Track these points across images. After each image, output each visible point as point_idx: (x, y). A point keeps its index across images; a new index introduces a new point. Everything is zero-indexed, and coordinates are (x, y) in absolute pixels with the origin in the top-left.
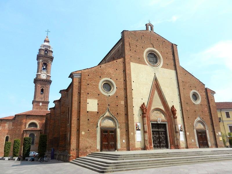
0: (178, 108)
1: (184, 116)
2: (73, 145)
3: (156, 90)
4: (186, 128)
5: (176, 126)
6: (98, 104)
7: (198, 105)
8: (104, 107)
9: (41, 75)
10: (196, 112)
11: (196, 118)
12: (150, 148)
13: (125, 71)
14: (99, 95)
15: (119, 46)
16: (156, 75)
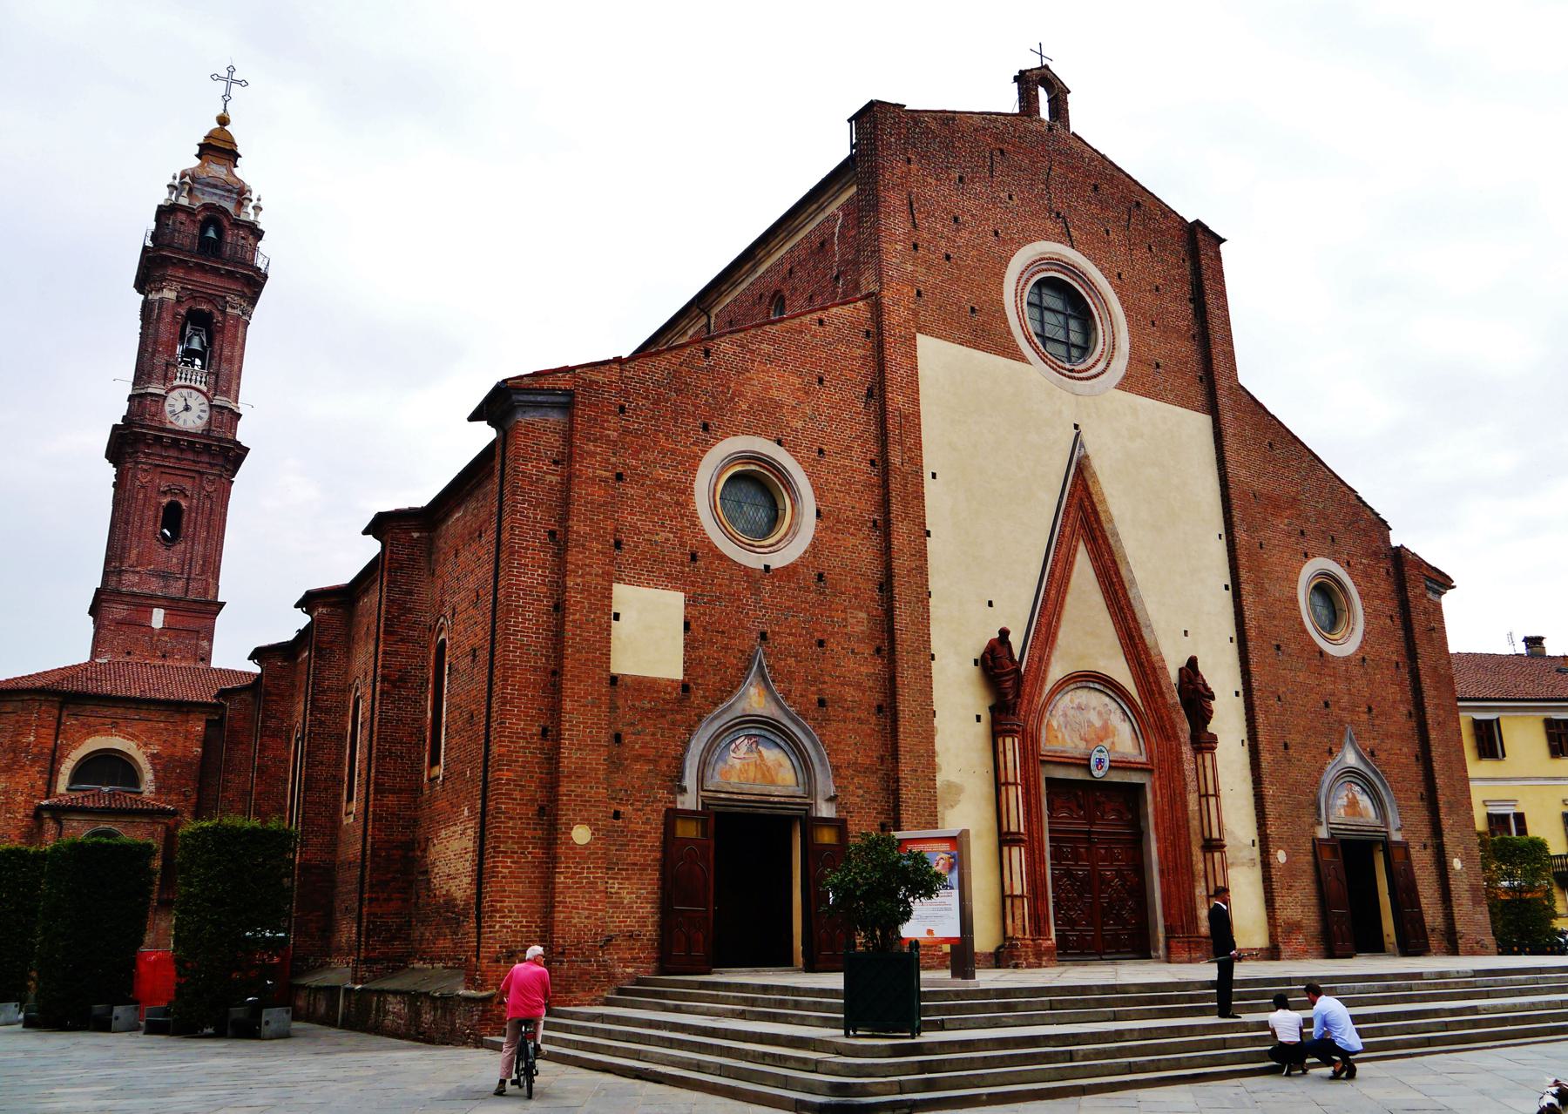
0: (1222, 677)
1: (1262, 737)
2: (508, 922)
3: (1082, 548)
4: (1270, 820)
5: (1212, 801)
6: (687, 626)
7: (1347, 660)
8: (726, 648)
9: (169, 401)
10: (1334, 709)
11: (1330, 752)
12: (1039, 954)
13: (876, 393)
14: (694, 557)
15: (833, 208)
16: (1086, 437)
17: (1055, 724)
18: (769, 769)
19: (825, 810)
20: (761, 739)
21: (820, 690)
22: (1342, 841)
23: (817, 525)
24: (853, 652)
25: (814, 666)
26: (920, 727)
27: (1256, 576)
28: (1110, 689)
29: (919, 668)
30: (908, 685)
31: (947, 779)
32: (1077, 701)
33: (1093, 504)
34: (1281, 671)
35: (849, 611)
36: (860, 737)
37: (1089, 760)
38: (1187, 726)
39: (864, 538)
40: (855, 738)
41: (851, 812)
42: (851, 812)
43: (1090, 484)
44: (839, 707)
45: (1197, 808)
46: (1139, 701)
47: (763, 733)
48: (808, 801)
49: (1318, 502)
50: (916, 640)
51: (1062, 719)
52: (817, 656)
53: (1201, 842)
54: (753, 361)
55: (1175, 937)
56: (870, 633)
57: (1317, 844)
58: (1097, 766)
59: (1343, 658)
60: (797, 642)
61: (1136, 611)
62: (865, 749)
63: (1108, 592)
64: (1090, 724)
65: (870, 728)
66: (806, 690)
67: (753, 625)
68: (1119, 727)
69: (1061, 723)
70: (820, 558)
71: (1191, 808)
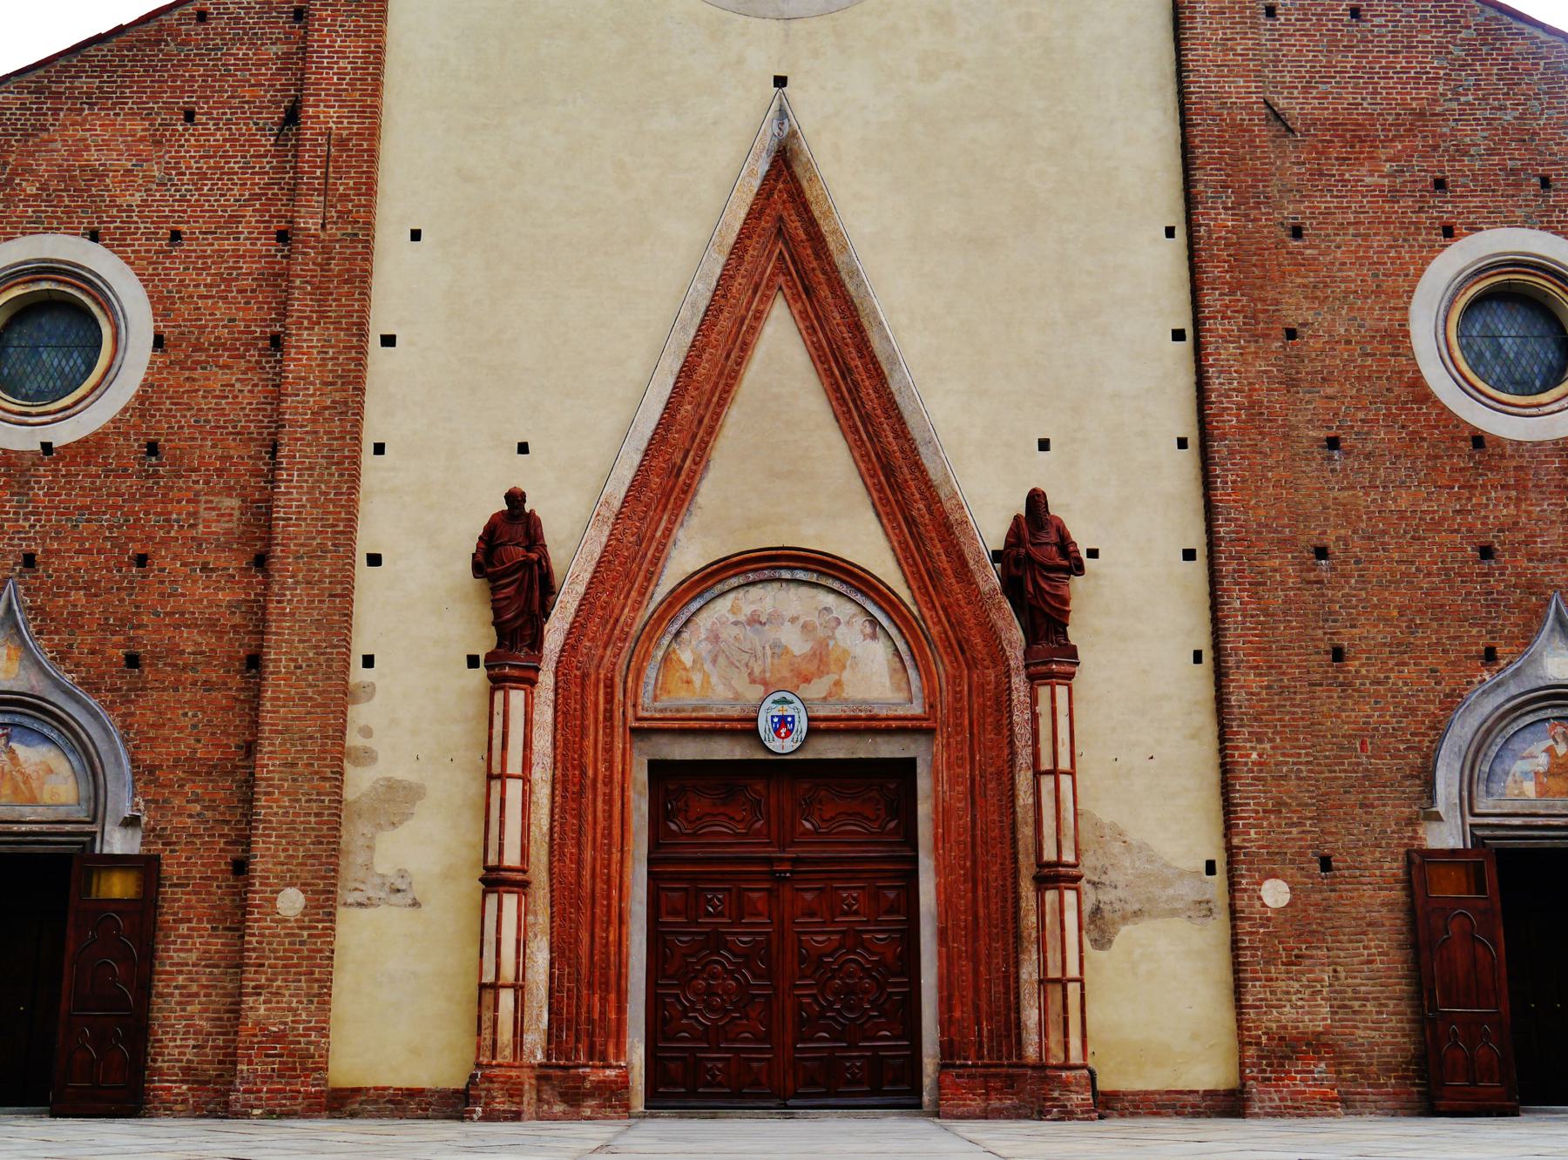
11: (1490, 656)
17: (686, 657)
18: (27, 779)
19: (119, 842)
20: (18, 729)
21: (131, 639)
22: (1501, 853)
23: (152, 362)
24: (205, 568)
25: (122, 600)
28: (835, 578)
32: (747, 610)
33: (811, 224)
34: (1336, 493)
35: (203, 498)
36: (204, 712)
37: (756, 720)
38: (1017, 635)
39: (248, 369)
40: (195, 716)
41: (175, 843)
42: (175, 843)
43: (805, 184)
44: (165, 664)
45: (1030, 801)
46: (905, 594)
47: (17, 719)
48: (87, 828)
49: (1502, 108)
51: (705, 647)
52: (130, 582)
53: (1034, 870)
54: (56, 111)
55: (954, 1066)
56: (244, 532)
57: (1421, 863)
58: (777, 732)
59: (1556, 442)
60: (93, 563)
62: (213, 734)
63: (839, 387)
64: (779, 650)
65: (226, 697)
66: (102, 642)
67: (9, 545)
68: (858, 651)
69: (704, 654)
70: (154, 416)
71: (1020, 802)
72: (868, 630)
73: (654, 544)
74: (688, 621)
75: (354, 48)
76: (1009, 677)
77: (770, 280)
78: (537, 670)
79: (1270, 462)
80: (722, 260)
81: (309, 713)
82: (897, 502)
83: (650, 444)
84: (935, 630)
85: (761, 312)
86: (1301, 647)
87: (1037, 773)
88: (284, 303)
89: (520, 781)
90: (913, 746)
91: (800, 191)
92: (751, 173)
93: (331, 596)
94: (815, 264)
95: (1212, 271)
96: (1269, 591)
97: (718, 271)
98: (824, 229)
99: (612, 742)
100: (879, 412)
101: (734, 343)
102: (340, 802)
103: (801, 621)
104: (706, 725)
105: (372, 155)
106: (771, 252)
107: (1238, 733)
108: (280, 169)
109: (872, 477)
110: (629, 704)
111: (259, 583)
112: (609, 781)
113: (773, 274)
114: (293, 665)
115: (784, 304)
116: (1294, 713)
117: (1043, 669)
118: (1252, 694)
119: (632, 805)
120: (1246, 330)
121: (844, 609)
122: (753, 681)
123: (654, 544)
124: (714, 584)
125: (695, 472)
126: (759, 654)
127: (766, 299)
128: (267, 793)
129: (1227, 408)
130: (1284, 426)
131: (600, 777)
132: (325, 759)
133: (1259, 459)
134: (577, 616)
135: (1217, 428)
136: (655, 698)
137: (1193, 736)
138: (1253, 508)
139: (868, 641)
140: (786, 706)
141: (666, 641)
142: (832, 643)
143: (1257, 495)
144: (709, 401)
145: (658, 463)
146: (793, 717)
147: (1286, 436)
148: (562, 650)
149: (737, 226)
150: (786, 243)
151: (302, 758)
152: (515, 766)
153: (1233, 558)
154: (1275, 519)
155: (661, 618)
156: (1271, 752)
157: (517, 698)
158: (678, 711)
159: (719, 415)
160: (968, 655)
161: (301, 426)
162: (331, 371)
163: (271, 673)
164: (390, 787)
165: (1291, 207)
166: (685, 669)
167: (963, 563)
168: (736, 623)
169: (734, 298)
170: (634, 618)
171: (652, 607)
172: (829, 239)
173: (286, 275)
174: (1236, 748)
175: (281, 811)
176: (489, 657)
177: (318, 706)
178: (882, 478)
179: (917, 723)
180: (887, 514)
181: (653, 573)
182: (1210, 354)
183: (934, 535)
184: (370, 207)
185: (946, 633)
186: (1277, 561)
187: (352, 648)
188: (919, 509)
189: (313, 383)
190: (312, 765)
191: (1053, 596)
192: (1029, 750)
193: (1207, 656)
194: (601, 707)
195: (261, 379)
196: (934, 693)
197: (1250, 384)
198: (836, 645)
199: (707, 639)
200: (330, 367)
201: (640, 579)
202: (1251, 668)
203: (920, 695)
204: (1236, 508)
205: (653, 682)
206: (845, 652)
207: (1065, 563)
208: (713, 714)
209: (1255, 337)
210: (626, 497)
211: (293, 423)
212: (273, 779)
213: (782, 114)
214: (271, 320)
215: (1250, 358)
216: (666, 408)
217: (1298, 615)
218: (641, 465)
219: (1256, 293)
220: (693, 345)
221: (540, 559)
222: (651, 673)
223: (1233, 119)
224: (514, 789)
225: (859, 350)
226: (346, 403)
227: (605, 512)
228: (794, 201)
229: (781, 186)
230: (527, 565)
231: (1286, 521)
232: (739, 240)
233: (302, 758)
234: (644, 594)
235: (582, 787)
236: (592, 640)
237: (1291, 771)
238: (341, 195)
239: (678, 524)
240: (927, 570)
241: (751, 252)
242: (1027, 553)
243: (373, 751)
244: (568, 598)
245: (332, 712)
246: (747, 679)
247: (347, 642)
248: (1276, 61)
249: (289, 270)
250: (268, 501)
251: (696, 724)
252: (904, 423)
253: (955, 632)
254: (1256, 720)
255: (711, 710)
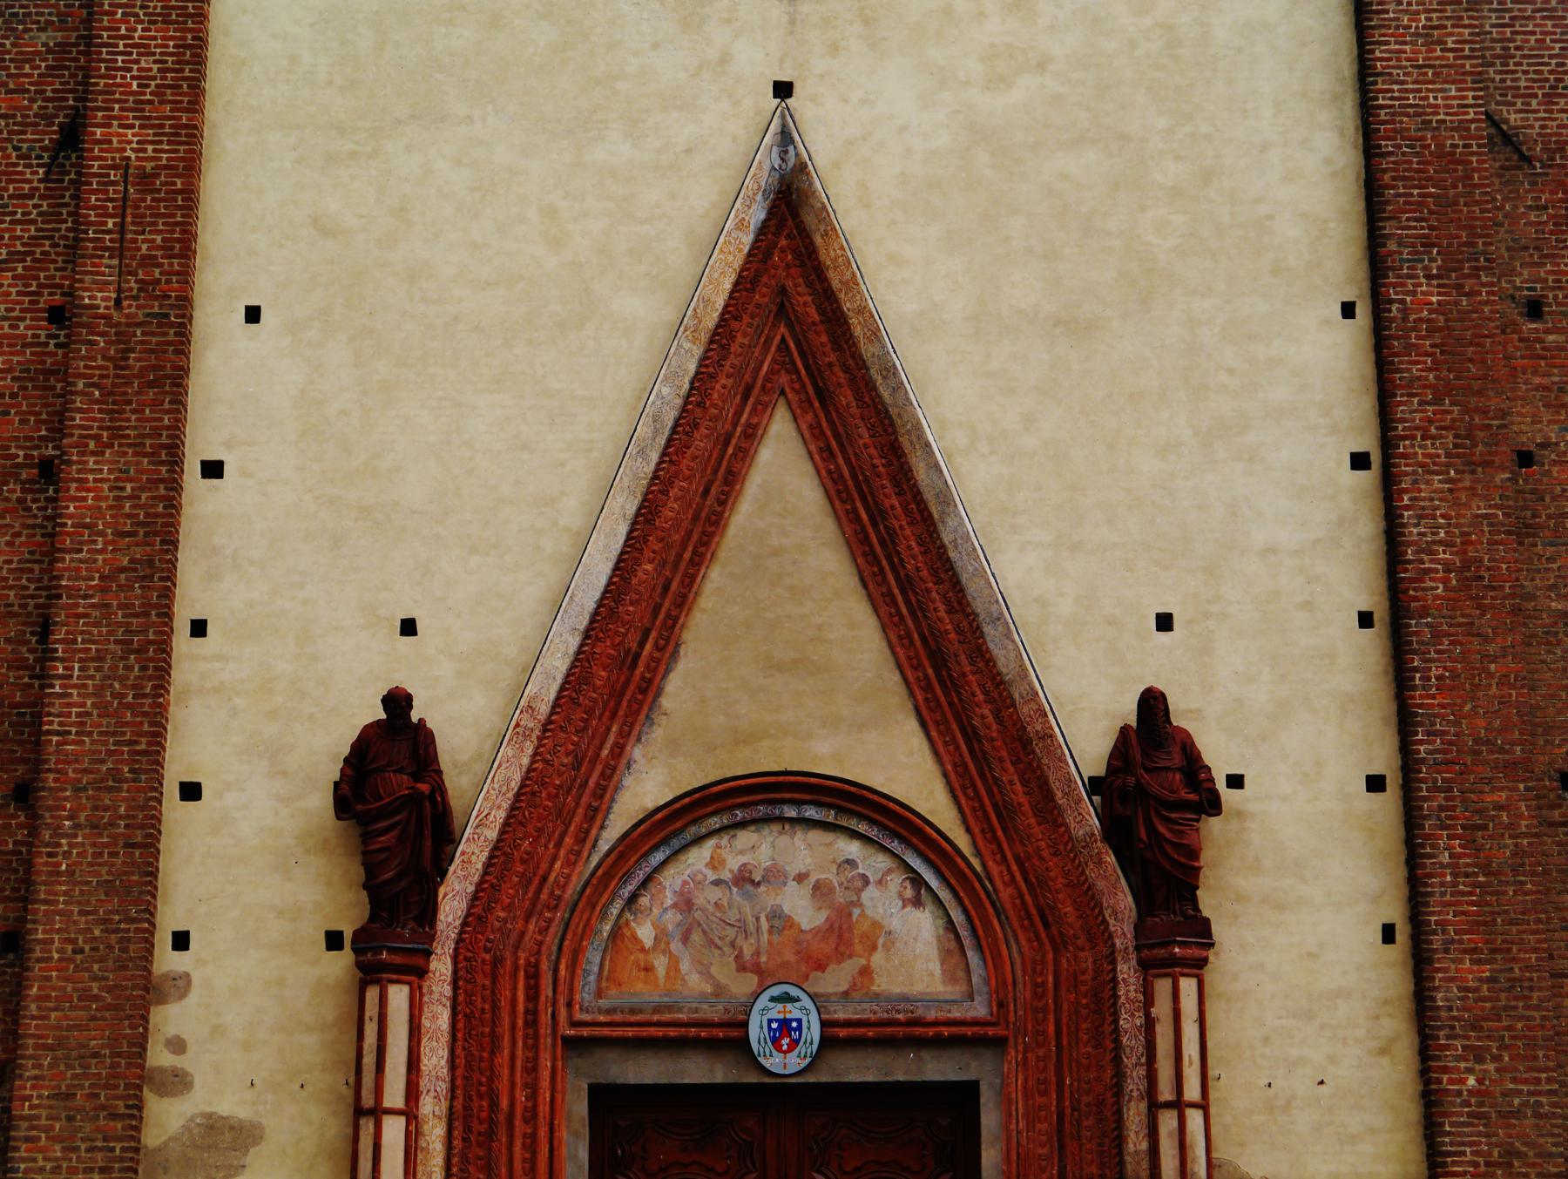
17: (645, 932)
26: (95, 978)
27: (1466, 410)
28: (861, 817)
29: (112, 825)
30: (70, 873)
31: (209, 1109)
32: (734, 863)
37: (744, 1025)
38: (1125, 901)
43: (818, 240)
45: (1144, 1146)
46: (962, 841)
50: (110, 753)
51: (671, 919)
58: (776, 1043)
61: (964, 578)
63: (866, 540)
64: (780, 921)
68: (895, 924)
71: (1131, 1148)
72: (909, 893)
73: (599, 768)
74: (648, 879)
75: (164, 41)
76: (1114, 962)
77: (767, 379)
78: (428, 954)
79: (1492, 649)
80: (698, 351)
81: (93, 1018)
82: (951, 704)
83: (592, 621)
84: (1006, 894)
85: (755, 427)
86: (1539, 921)
87: (1154, 1107)
88: (61, 413)
89: (402, 1121)
90: (974, 1064)
91: (812, 250)
92: (741, 225)
93: (128, 845)
94: (832, 358)
95: (1412, 368)
96: (1491, 837)
97: (692, 367)
98: (847, 306)
99: (536, 1059)
100: (925, 574)
101: (715, 472)
102: (137, 1150)
103: (812, 879)
104: (673, 1032)
105: (188, 200)
106: (769, 340)
107: (1447, 1047)
108: (53, 216)
109: (915, 668)
110: (562, 1001)
111: (20, 826)
112: (531, 1116)
113: (771, 371)
114: (70, 947)
115: (788, 415)
116: (1528, 1018)
117: (1161, 952)
118: (1467, 989)
119: (565, 1151)
120: (1458, 456)
121: (874, 863)
122: (742, 968)
123: (599, 768)
124: (686, 826)
125: (658, 661)
126: (751, 928)
127: (763, 409)
128: (28, 1139)
129: (1430, 570)
130: (1512, 596)
131: (518, 1116)
132: (116, 1087)
133: (1476, 644)
134: (486, 873)
135: (1416, 599)
136: (599, 993)
137: (1383, 1052)
138: (1468, 716)
139: (909, 909)
140: (789, 1006)
141: (615, 910)
142: (856, 912)
143: (1473, 698)
144: (679, 556)
145: (605, 648)
146: (799, 1021)
147: (1516, 610)
148: (464, 924)
149: (720, 302)
150: (790, 326)
151: (81, 1087)
152: (394, 1095)
153: (1439, 790)
154: (1499, 732)
155: (608, 876)
156: (1495, 1076)
157: (398, 996)
158: (632, 1011)
159: (693, 578)
160: (1054, 929)
161: (86, 597)
162: (129, 516)
163: (39, 960)
164: (211, 1127)
165: (1525, 272)
166: (643, 950)
167: (1049, 796)
168: (717, 883)
169: (714, 406)
170: (569, 877)
171: (595, 860)
172: (853, 321)
173: (62, 372)
174: (1445, 1070)
175: (49, 1166)
176: (356, 934)
177: (108, 1007)
178: (930, 671)
179: (981, 1030)
180: (937, 723)
181: (596, 810)
182: (1406, 491)
183: (1005, 754)
184: (185, 276)
185: (1021, 897)
186: (1504, 795)
187: (158, 920)
188: (983, 717)
189: (102, 534)
190: (97, 1096)
191: (1176, 845)
192: (1142, 1071)
193: (1402, 934)
194: (521, 1007)
195: (24, 526)
196: (1005, 984)
197: (1463, 534)
198: (863, 914)
199: (675, 906)
200: (127, 510)
201: (577, 819)
202: (1465, 951)
203: (985, 989)
204: (1443, 717)
205: (596, 969)
206: (876, 924)
207: (1193, 797)
208: (683, 1016)
209: (1471, 465)
210: (558, 698)
211: (73, 592)
212: (38, 1117)
213: (786, 138)
214: (41, 438)
215: (1463, 497)
216: (616, 568)
217: (1534, 874)
218: (579, 651)
219: (1473, 401)
220: (655, 476)
221: (432, 793)
222: (593, 957)
223: (1440, 146)
224: (394, 1130)
225: (896, 484)
226: (151, 563)
227: (527, 722)
228: (802, 265)
229: (783, 242)
230: (415, 800)
231: (1517, 735)
232: (723, 321)
233: (81, 1087)
234: (584, 841)
235: (492, 1123)
236: (506, 908)
237: (1525, 1104)
238: (144, 257)
239: (633, 738)
240: (995, 805)
241: (740, 339)
242: (1138, 783)
243: (186, 1074)
244: (473, 847)
245: (129, 1017)
246: (733, 966)
247: (150, 912)
248: (1506, 57)
249: (67, 365)
250: (34, 705)
251: (659, 1032)
252: (962, 590)
253: (1034, 896)
254: (1473, 1028)
255: (680, 1010)
